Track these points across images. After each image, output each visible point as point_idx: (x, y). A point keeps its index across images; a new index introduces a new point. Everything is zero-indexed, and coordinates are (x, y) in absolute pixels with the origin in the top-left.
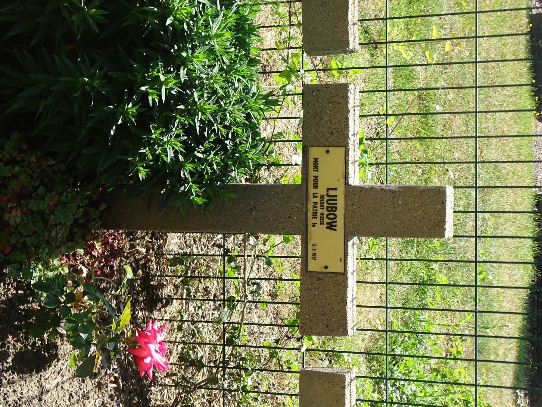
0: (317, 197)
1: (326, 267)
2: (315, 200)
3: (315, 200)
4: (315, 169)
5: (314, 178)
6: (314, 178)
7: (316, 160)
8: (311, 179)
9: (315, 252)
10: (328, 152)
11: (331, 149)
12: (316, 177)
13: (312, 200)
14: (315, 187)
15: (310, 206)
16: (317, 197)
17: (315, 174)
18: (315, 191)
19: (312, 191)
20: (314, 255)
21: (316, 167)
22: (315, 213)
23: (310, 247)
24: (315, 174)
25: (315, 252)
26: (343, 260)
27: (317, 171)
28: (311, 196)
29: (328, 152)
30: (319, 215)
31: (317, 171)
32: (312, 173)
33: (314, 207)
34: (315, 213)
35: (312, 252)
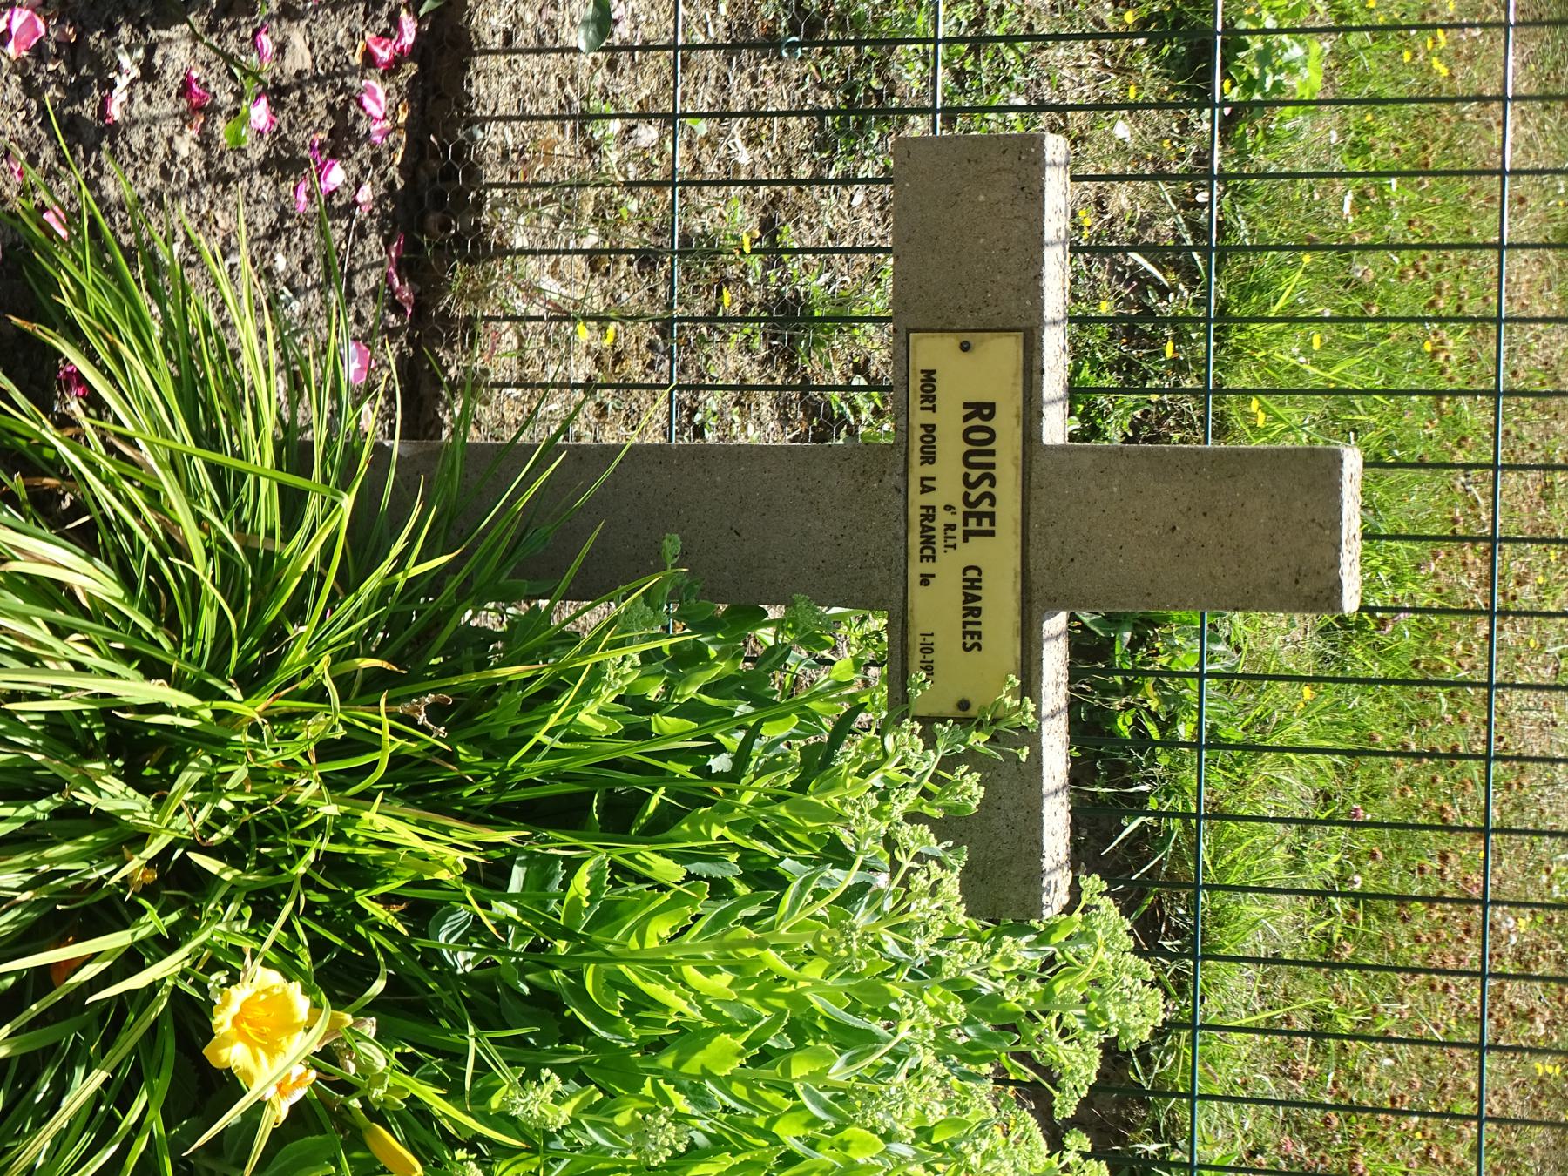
0: (933, 489)
1: (964, 705)
2: (928, 499)
3: (928, 499)
4: (927, 404)
5: (922, 432)
6: (922, 432)
7: (929, 376)
9: (929, 657)
12: (929, 429)
13: (917, 500)
14: (929, 458)
15: (915, 514)
16: (933, 489)
17: (928, 418)
18: (928, 470)
19: (917, 471)
21: (929, 398)
22: (928, 541)
23: (915, 641)
24: (928, 418)
25: (929, 657)
27: (933, 409)
28: (914, 487)
29: (965, 347)
30: (939, 544)
31: (933, 409)
32: (919, 417)
34: (928, 541)
35: (920, 656)
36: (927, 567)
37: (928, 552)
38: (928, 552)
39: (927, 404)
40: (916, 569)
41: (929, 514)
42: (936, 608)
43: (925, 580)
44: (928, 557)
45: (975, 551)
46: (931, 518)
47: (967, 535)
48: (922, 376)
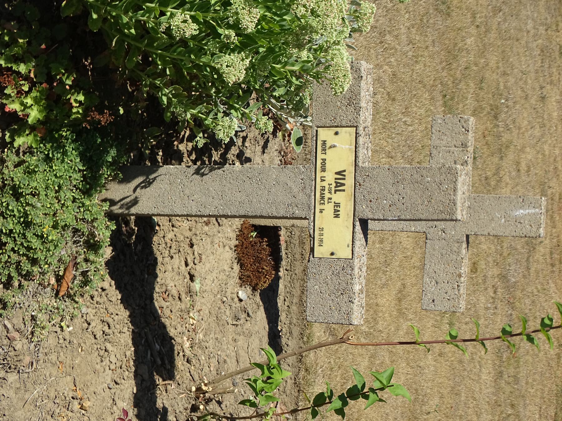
0: (324, 180)
2: (324, 184)
3: (324, 184)
4: (323, 152)
7: (324, 142)
8: (319, 162)
9: (322, 237)
10: (336, 133)
12: (324, 160)
14: (324, 170)
16: (324, 180)
17: (323, 156)
18: (323, 174)
20: (321, 240)
22: (322, 198)
24: (323, 156)
26: (351, 246)
27: (325, 153)
29: (336, 133)
30: (326, 200)
31: (325, 153)
32: (320, 156)
34: (322, 198)
36: (322, 207)
37: (322, 202)
38: (322, 202)
39: (323, 152)
40: (318, 207)
41: (323, 189)
43: (321, 211)
44: (322, 203)
45: (338, 197)
46: (324, 190)
47: (336, 191)
48: (322, 142)
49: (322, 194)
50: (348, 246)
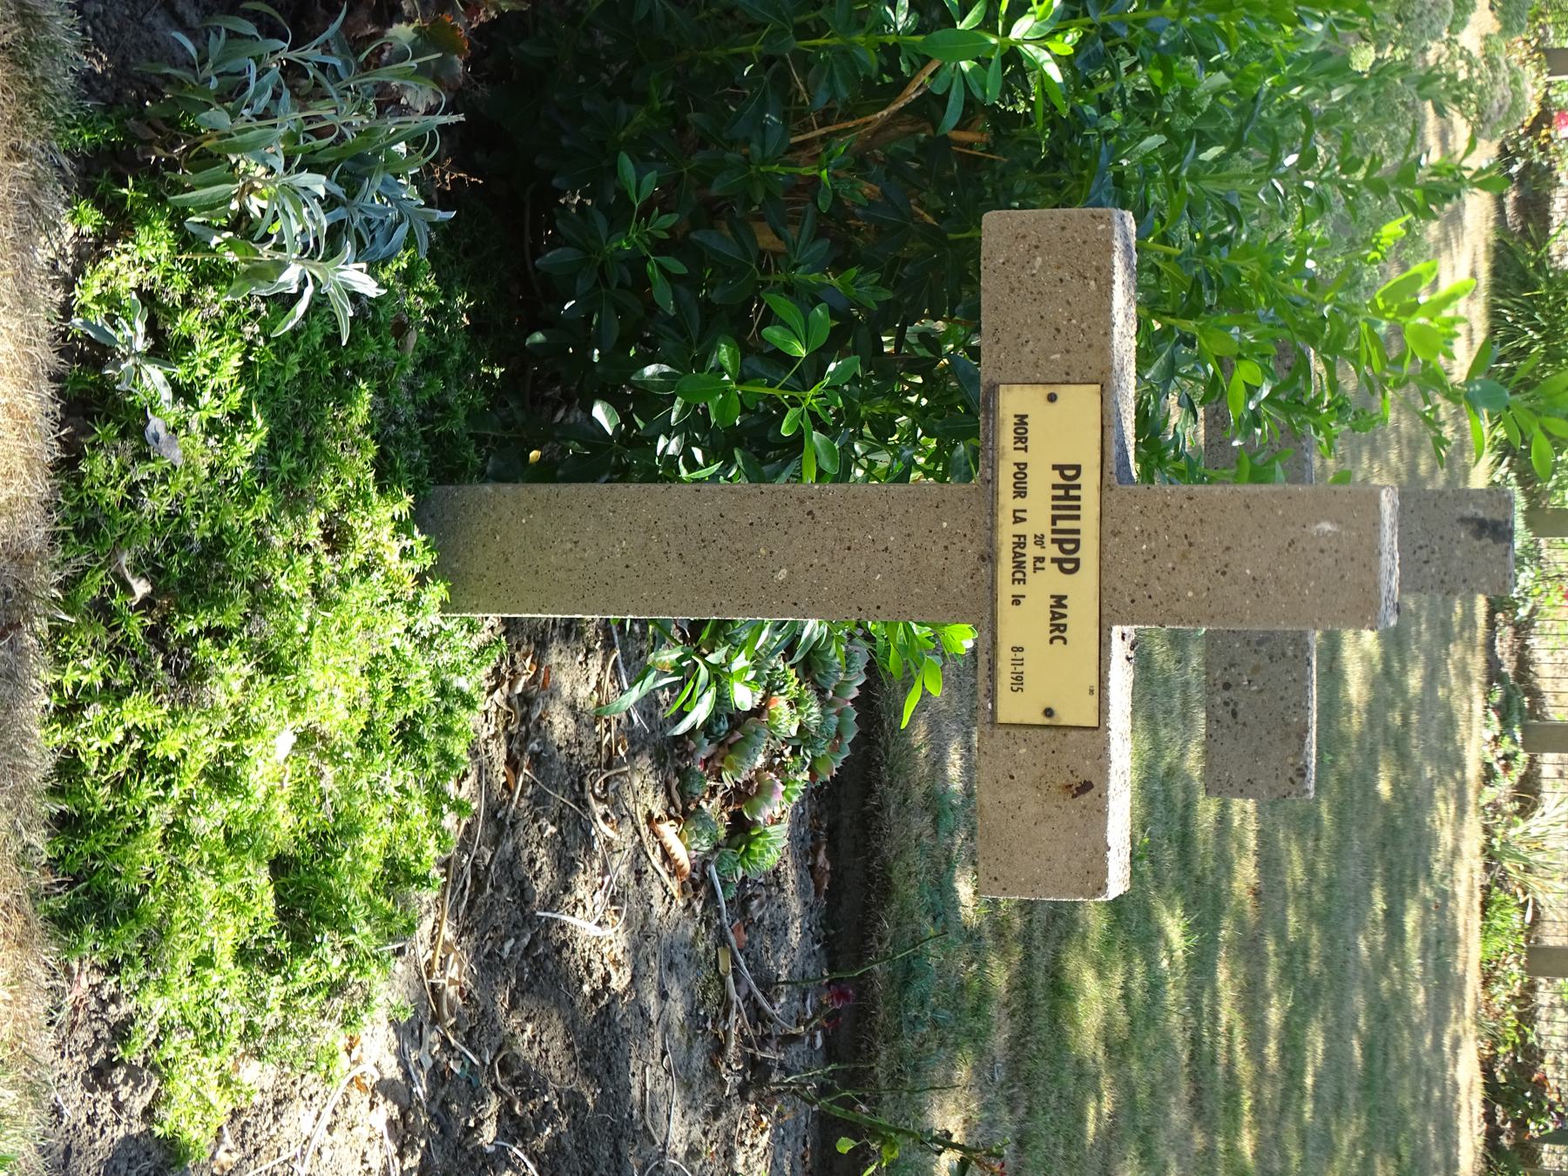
1: (1049, 712)
2: (1020, 529)
3: (1020, 529)
4: (1019, 445)
5: (1015, 469)
6: (1015, 469)
7: (1022, 420)
9: (1019, 669)
10: (1052, 398)
11: (1063, 391)
12: (1021, 467)
14: (1020, 493)
17: (1020, 457)
19: (1007, 501)
20: (1018, 679)
21: (1021, 438)
22: (1019, 566)
24: (1020, 457)
25: (1019, 669)
27: (1026, 449)
28: (1005, 518)
31: (1026, 449)
33: (1018, 545)
34: (1019, 566)
36: (1018, 589)
37: (1019, 576)
40: (1006, 589)
42: (1022, 625)
43: (1016, 601)
49: (1016, 555)
50: (1092, 692)
